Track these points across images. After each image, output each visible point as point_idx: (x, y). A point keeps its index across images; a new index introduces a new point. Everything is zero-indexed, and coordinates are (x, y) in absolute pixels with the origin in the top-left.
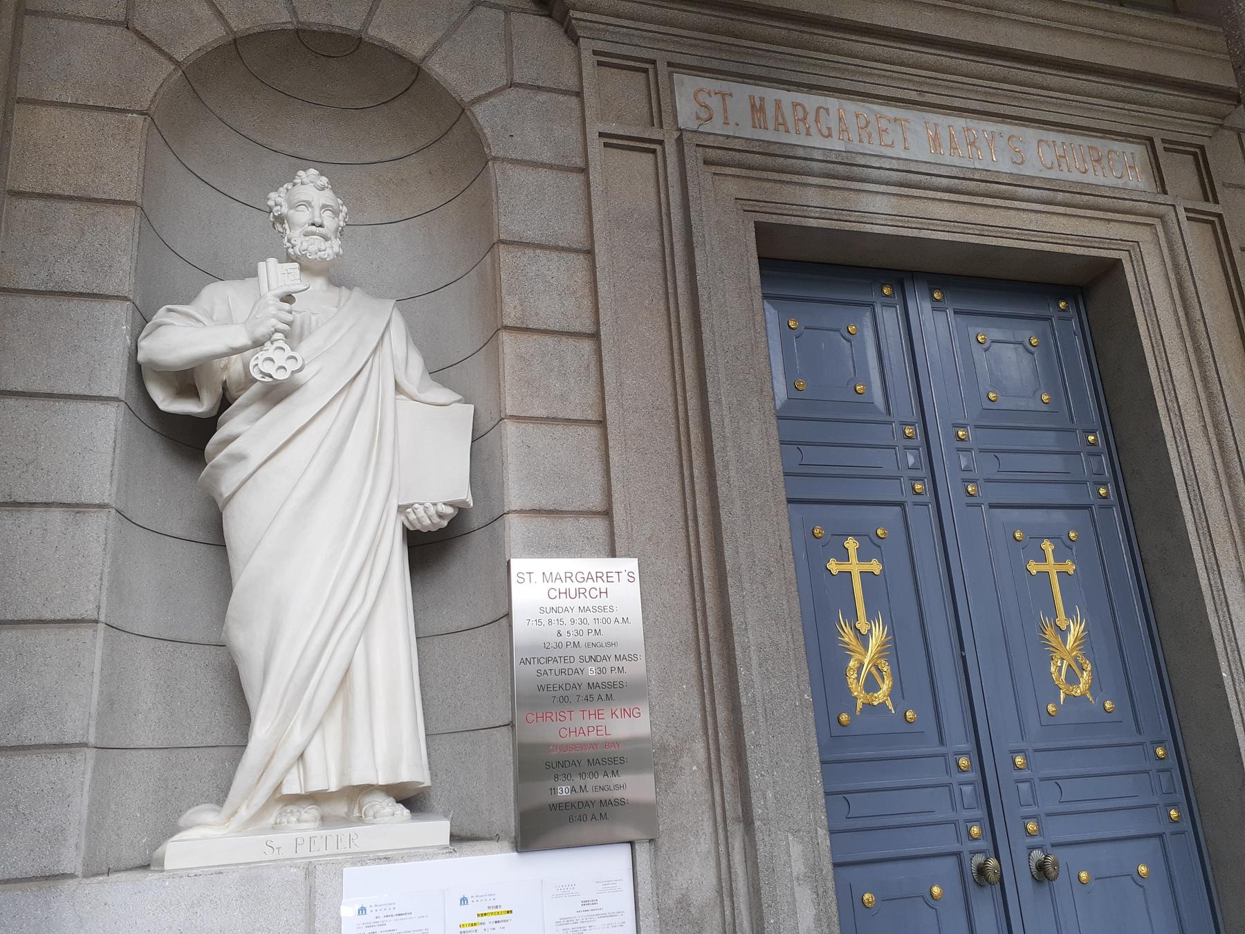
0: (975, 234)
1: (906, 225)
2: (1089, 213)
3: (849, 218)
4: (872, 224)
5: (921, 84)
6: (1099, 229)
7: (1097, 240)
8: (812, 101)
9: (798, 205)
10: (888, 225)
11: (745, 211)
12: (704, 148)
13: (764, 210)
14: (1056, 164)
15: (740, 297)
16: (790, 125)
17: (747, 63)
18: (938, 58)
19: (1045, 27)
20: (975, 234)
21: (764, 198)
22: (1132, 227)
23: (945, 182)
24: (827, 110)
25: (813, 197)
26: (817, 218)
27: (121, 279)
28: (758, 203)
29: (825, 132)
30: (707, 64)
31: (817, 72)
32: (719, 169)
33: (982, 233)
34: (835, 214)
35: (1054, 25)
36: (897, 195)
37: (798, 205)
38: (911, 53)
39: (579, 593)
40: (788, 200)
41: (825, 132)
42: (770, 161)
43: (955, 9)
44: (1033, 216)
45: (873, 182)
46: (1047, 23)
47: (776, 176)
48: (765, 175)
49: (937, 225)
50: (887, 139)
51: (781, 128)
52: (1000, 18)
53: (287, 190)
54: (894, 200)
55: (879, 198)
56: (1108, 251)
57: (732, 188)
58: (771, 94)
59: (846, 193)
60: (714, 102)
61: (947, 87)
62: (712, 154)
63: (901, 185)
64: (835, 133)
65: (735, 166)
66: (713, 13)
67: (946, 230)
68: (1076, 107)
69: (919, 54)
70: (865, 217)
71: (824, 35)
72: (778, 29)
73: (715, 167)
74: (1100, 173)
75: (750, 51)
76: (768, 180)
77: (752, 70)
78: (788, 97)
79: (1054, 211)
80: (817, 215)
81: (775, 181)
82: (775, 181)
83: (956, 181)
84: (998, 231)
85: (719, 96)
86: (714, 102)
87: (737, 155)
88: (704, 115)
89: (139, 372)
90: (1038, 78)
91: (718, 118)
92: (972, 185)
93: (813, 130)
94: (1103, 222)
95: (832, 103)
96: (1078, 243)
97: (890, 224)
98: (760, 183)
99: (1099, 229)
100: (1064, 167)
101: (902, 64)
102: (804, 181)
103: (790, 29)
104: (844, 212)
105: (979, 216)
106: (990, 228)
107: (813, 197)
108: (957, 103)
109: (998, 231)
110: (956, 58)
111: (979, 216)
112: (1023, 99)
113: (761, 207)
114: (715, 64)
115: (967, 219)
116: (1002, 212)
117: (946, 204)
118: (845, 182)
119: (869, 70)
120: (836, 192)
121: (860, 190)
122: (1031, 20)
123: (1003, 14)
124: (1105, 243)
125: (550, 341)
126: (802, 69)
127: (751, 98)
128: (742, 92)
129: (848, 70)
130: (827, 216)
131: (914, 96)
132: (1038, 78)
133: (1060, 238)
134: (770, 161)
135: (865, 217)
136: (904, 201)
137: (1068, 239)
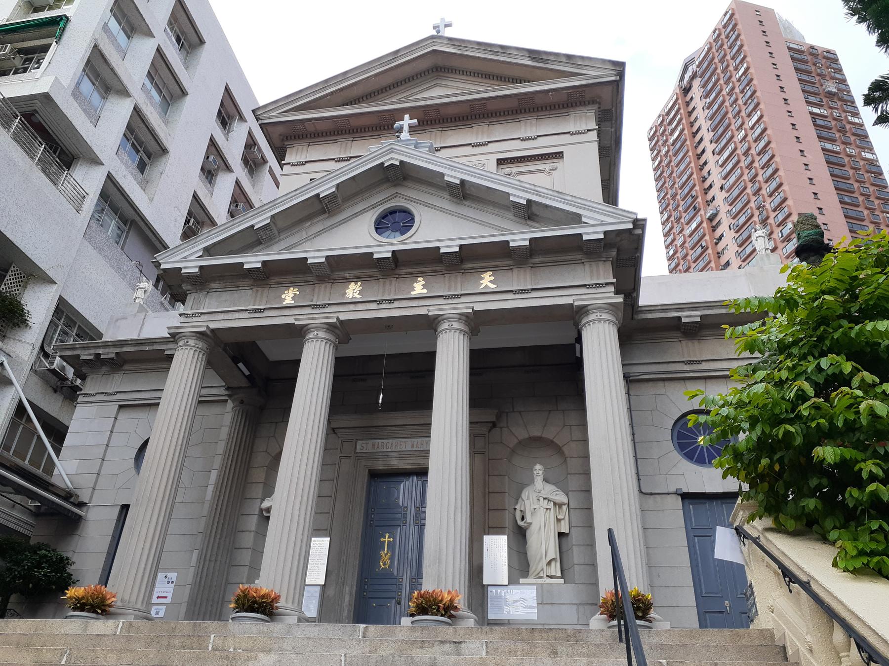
8: (385, 441)
27: (260, 496)
39: (319, 544)
58: (377, 441)
78: (380, 441)
86: (364, 445)
89: (261, 510)
91: (365, 449)
125: (323, 498)
128: (371, 442)
131: (409, 436)
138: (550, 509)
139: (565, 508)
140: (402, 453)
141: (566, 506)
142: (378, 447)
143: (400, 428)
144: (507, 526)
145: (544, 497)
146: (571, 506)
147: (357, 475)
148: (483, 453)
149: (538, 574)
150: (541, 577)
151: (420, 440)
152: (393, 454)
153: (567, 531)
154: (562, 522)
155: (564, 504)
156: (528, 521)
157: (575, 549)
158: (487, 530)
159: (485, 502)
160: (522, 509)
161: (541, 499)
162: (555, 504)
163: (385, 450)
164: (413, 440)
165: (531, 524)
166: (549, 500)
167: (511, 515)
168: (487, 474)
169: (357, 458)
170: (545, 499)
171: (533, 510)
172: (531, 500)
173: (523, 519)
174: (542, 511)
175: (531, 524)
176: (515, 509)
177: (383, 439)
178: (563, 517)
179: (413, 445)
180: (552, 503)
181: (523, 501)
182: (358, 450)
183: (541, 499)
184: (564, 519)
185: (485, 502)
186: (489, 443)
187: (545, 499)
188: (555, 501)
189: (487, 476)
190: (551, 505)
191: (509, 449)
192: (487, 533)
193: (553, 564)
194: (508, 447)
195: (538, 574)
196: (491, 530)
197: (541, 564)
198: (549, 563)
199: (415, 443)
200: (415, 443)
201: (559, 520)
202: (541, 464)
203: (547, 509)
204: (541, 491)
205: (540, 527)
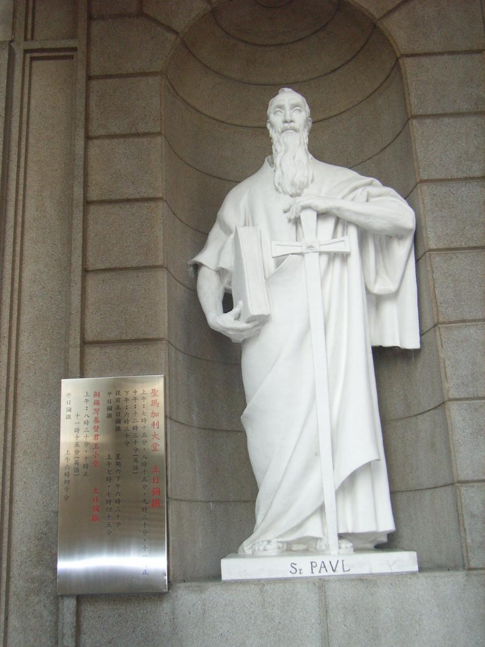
138: (344, 257)
139: (402, 250)
141: (408, 243)
144: (162, 331)
145: (323, 205)
146: (432, 240)
148: (65, 54)
149: (299, 526)
150: (308, 546)
153: (412, 342)
154: (389, 310)
155: (396, 235)
156: (255, 310)
157: (457, 414)
158: (74, 354)
159: (69, 241)
160: (227, 262)
161: (308, 217)
162: (364, 235)
165: (261, 321)
166: (338, 220)
167: (181, 293)
168: (81, 133)
170: (322, 215)
171: (271, 263)
172: (263, 226)
173: (228, 303)
174: (314, 263)
175: (261, 321)
176: (197, 267)
178: (393, 288)
180: (353, 232)
181: (227, 230)
183: (308, 217)
184: (394, 296)
185: (69, 241)
186: (90, 18)
187: (322, 215)
188: (362, 220)
189: (80, 143)
190: (349, 241)
191: (171, 37)
192: (76, 367)
193: (363, 487)
194: (169, 29)
195: (299, 526)
196: (93, 353)
197: (312, 484)
198: (348, 485)
201: (375, 301)
202: (296, 86)
203: (332, 256)
204: (303, 186)
205: (307, 329)
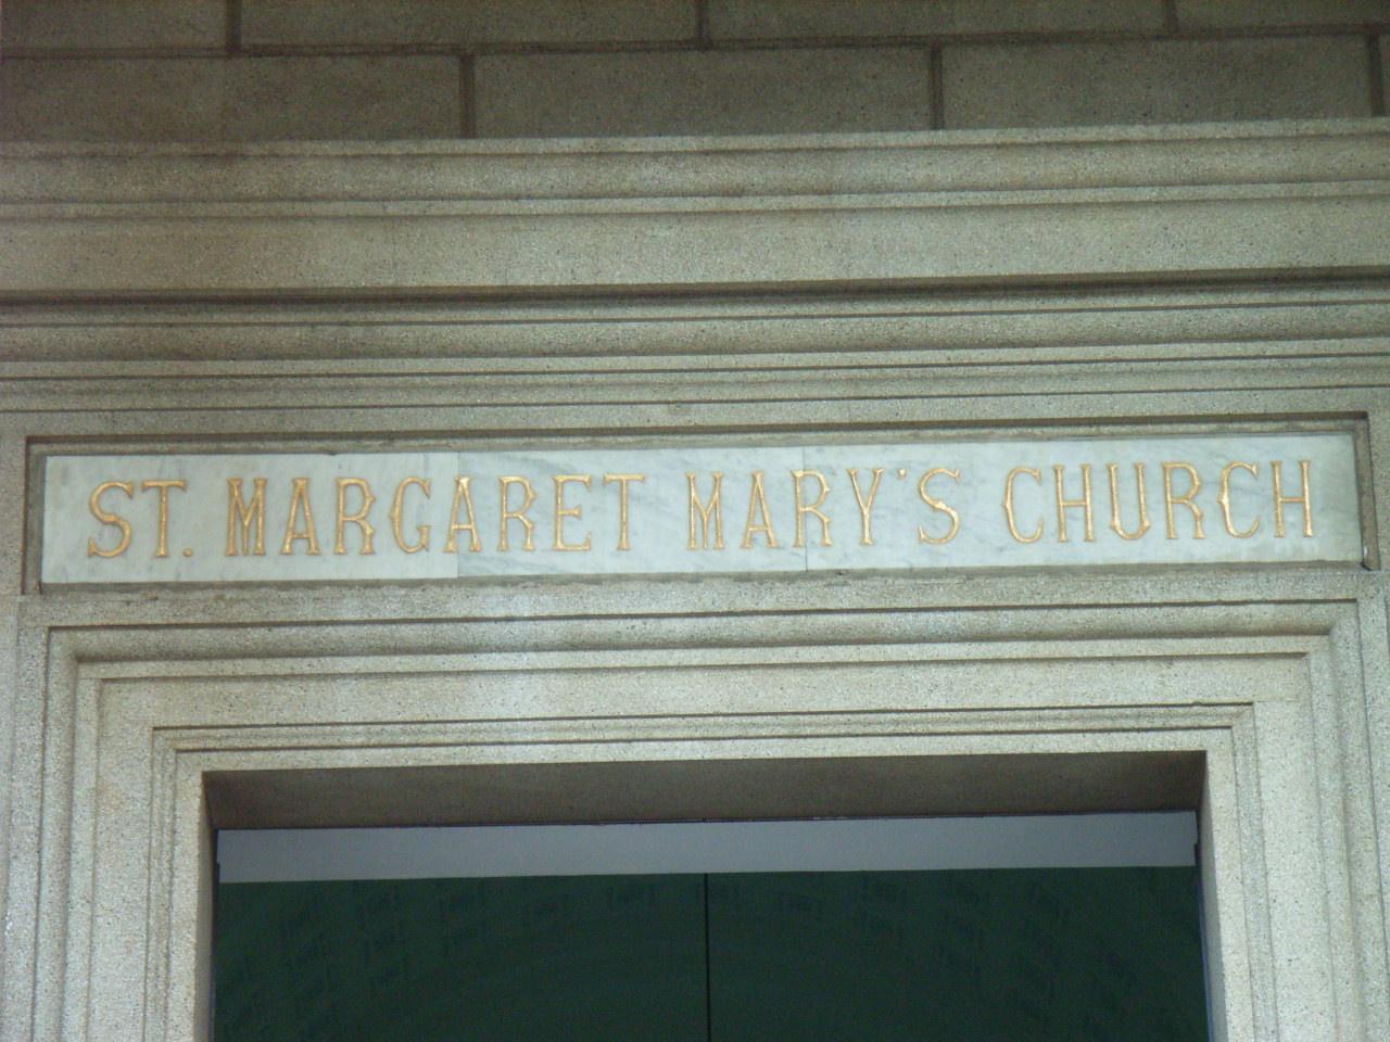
0: (780, 737)
1: (589, 738)
2: (1105, 647)
3: (441, 738)
4: (501, 743)
5: (673, 386)
6: (1143, 685)
7: (1128, 711)
9: (310, 725)
10: (545, 743)
11: (179, 751)
12: (72, 633)
13: (225, 744)
14: (1052, 525)
15: (129, 952)
16: (325, 532)
17: (224, 409)
18: (703, 325)
19: (983, 209)
20: (780, 737)
21: (227, 719)
22: (1238, 666)
23: (681, 628)
24: (426, 489)
25: (347, 703)
26: (362, 747)
28: (212, 732)
29: (411, 536)
30: (127, 426)
31: (402, 402)
32: (115, 670)
33: (796, 731)
34: (404, 732)
35: (1004, 198)
36: (567, 670)
37: (310, 725)
38: (634, 324)
40: (287, 716)
41: (411, 536)
42: (230, 638)
43: (727, 213)
44: (942, 674)
45: (500, 649)
46: (986, 198)
47: (256, 666)
48: (228, 667)
49: (669, 727)
50: (574, 533)
51: (301, 545)
52: (853, 211)
53: (261, 191)
54: (560, 683)
55: (520, 682)
56: (1168, 736)
57: (144, 705)
58: (281, 468)
59: (436, 683)
60: (139, 511)
61: (743, 384)
62: (92, 642)
63: (574, 647)
64: (438, 540)
65: (153, 658)
66: (122, 319)
67: (697, 735)
68: (1118, 373)
69: (652, 326)
70: (480, 732)
71: (401, 323)
72: (287, 328)
73: (107, 665)
74: (1184, 528)
75: (225, 383)
76: (235, 678)
77: (233, 423)
79: (999, 655)
80: (359, 740)
81: (255, 678)
82: (255, 678)
83: (714, 621)
84: (837, 724)
85: (153, 493)
87: (153, 637)
88: (108, 540)
90: (991, 326)
91: (144, 545)
92: (756, 626)
93: (383, 539)
94: (1151, 665)
95: (443, 465)
96: (1073, 725)
97: (547, 739)
98: (217, 687)
99: (1143, 685)
100: (1076, 529)
101: (613, 352)
102: (325, 670)
103: (313, 325)
104: (428, 727)
105: (791, 692)
106: (815, 718)
107: (347, 703)
108: (776, 415)
109: (837, 724)
110: (751, 318)
111: (791, 692)
112: (961, 378)
113: (220, 740)
114: (148, 422)
115: (752, 704)
116: (854, 675)
117: (697, 675)
118: (428, 657)
119: (530, 379)
120: (409, 683)
121: (468, 673)
122: (941, 199)
123: (860, 201)
124: (1153, 716)
126: (361, 401)
127: (234, 485)
128: (211, 474)
129: (476, 387)
130: (387, 740)
131: (660, 416)
132: (991, 326)
133: (1020, 720)
134: (230, 638)
135: (480, 732)
136: (588, 683)
137: (1040, 719)
140: (595, 602)
142: (302, 537)
143: (549, 328)
147: (82, 836)
151: (783, 461)
152: (493, 603)
163: (389, 565)
164: (710, 459)
169: (61, 645)
177: (360, 439)
179: (706, 522)
182: (61, 560)
199: (736, 494)
200: (736, 494)
